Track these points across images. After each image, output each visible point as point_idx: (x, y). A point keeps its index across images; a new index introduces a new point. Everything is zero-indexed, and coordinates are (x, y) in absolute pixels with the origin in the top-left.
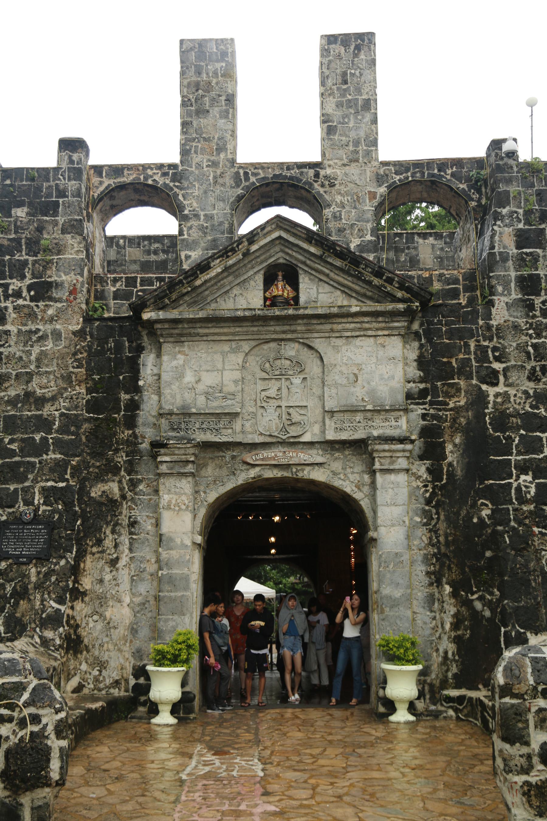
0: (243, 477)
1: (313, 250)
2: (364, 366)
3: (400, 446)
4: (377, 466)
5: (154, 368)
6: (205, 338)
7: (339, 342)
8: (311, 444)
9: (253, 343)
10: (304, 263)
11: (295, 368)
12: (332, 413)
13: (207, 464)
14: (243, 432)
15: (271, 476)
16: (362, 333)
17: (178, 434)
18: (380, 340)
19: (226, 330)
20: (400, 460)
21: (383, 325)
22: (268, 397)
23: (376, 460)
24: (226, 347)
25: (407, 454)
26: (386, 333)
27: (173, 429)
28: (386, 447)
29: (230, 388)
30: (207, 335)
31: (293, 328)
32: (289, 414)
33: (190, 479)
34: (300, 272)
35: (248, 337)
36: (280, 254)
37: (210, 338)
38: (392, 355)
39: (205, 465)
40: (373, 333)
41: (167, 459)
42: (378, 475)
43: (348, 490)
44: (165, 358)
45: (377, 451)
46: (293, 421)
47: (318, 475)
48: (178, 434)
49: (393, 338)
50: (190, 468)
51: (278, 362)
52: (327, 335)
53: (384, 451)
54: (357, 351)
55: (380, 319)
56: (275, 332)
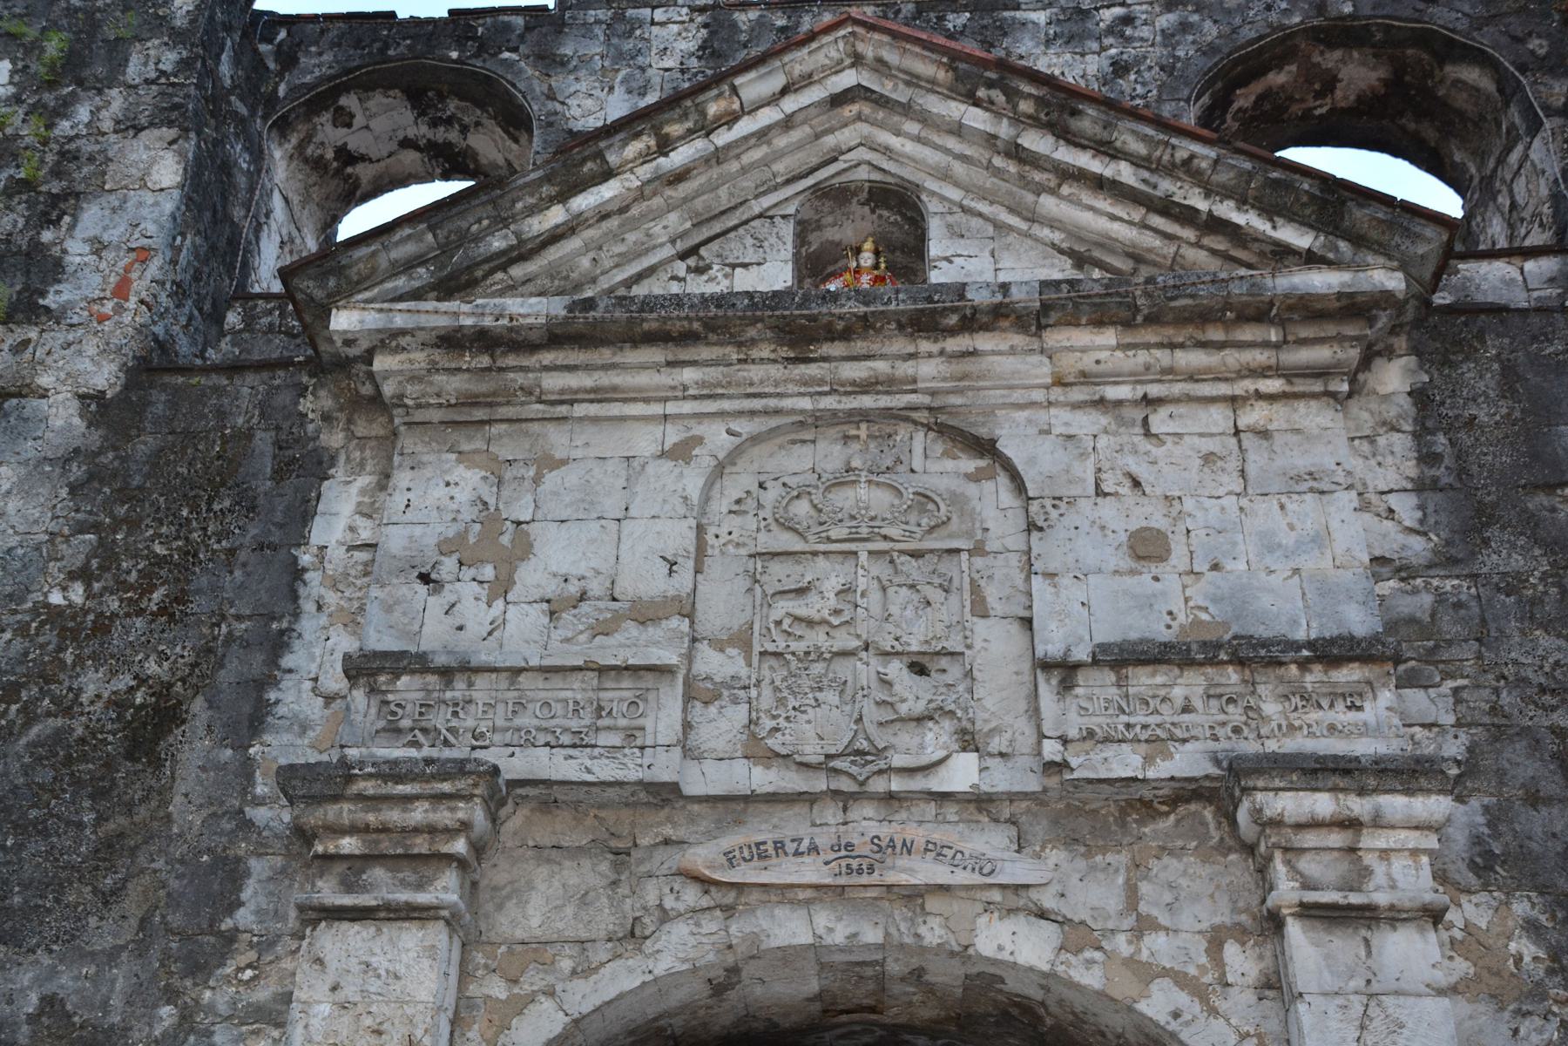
0: (680, 950)
1: (977, 118)
2: (1189, 504)
3: (1395, 804)
4: (1286, 891)
5: (361, 522)
6: (563, 410)
7: (1086, 423)
8: (980, 803)
9: (745, 427)
10: (945, 176)
11: (913, 518)
12: (1065, 671)
13: (530, 886)
14: (690, 753)
15: (805, 938)
16: (1178, 389)
17: (413, 753)
18: (1253, 416)
19: (644, 379)
20: (1399, 865)
21: (1260, 357)
22: (797, 619)
23: (1279, 867)
24: (645, 441)
25: (1432, 842)
26: (1273, 385)
27: (394, 730)
28: (1323, 804)
29: (646, 580)
30: (570, 398)
31: (905, 369)
32: (886, 683)
33: (437, 934)
34: (932, 206)
35: (726, 405)
36: (863, 154)
37: (580, 410)
38: (1301, 461)
39: (519, 892)
40: (1224, 389)
41: (349, 844)
42: (1294, 929)
43: (1158, 1004)
44: (402, 478)
45: (1277, 823)
46: (903, 709)
47: (1019, 947)
48: (413, 753)
49: (1301, 406)
50: (445, 889)
51: (845, 499)
52: (1038, 395)
53: (1315, 824)
54: (1158, 452)
55: (1247, 333)
56: (837, 388)
